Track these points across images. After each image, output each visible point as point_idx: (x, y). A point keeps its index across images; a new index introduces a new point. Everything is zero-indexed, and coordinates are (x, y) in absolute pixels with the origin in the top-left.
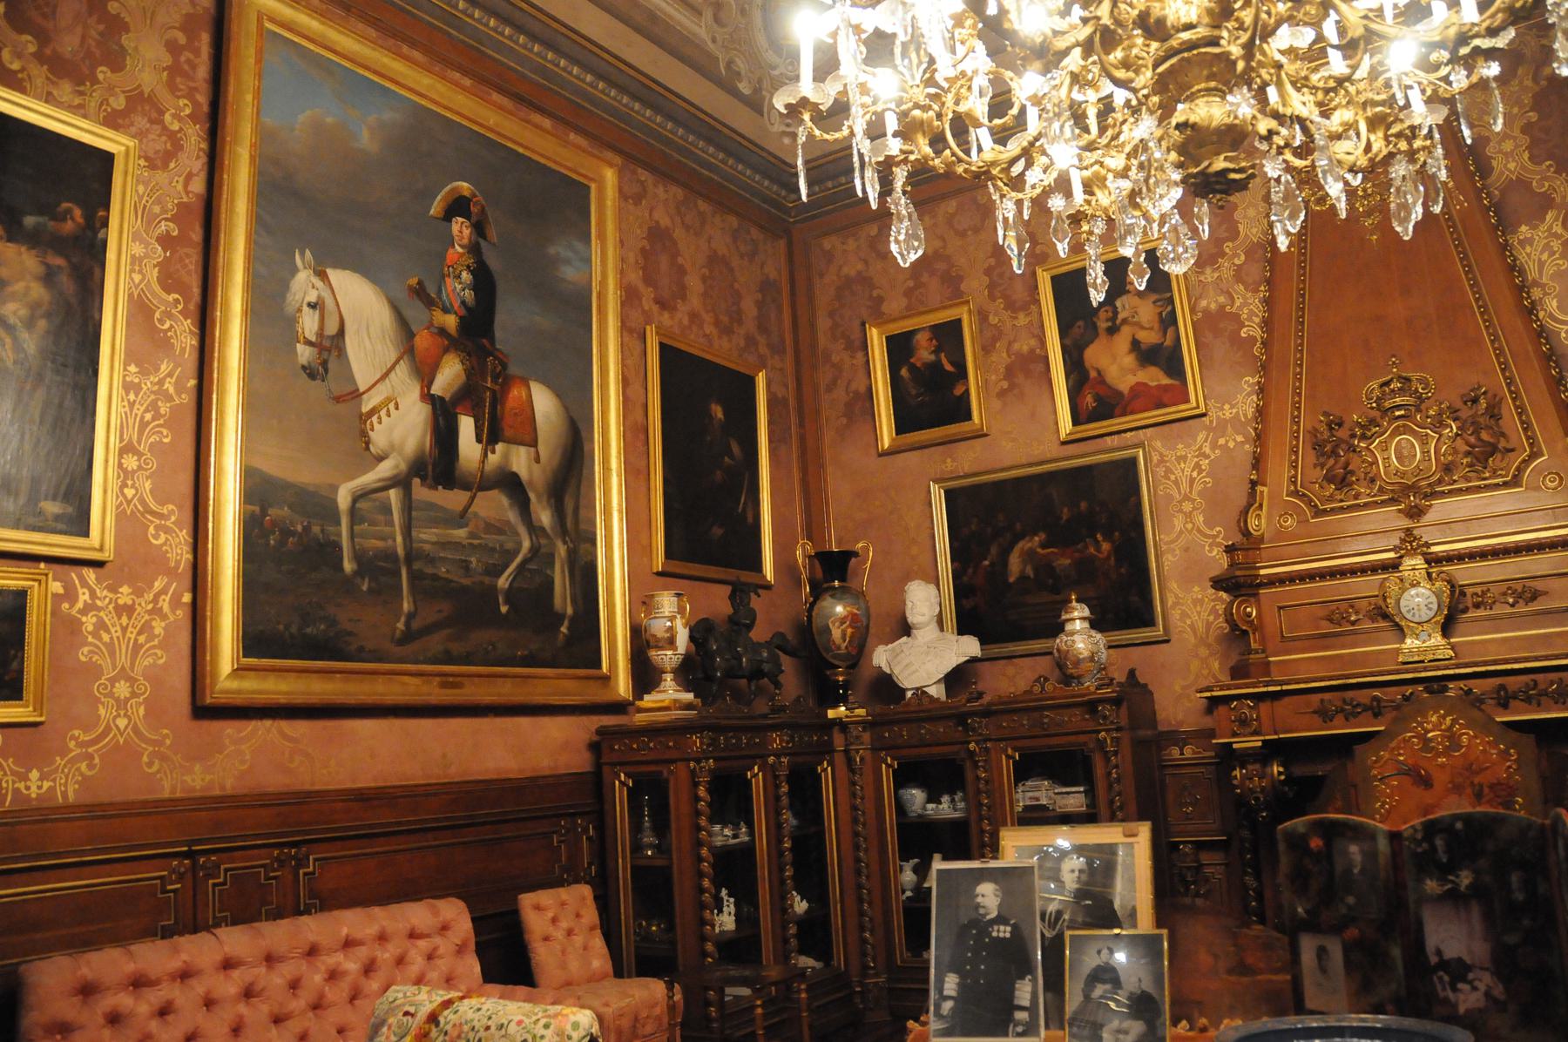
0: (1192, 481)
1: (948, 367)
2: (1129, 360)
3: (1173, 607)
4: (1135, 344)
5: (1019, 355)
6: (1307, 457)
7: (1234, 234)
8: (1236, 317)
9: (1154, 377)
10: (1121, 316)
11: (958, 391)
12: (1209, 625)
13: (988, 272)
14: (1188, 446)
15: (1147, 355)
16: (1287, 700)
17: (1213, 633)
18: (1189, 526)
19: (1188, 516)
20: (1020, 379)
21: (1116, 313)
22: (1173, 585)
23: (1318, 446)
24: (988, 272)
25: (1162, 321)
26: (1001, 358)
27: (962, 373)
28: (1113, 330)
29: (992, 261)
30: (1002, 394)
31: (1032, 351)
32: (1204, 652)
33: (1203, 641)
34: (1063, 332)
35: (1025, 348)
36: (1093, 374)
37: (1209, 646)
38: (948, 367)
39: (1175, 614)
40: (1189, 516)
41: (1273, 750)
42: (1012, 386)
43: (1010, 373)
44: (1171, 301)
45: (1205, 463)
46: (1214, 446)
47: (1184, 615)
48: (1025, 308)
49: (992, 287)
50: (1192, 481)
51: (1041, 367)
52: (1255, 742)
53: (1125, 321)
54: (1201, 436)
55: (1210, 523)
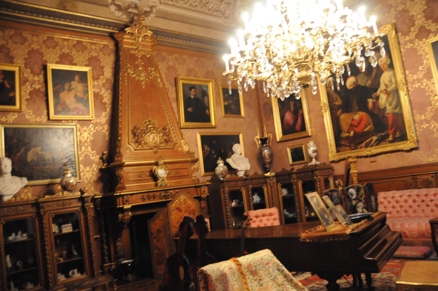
0: (88, 138)
1: (8, 86)
2: (74, 100)
3: (82, 172)
4: (76, 96)
5: (34, 88)
6: (131, 135)
7: (103, 75)
8: (102, 96)
9: (80, 106)
10: (72, 87)
11: (11, 95)
12: (91, 178)
13: (25, 59)
14: (87, 127)
15: (78, 99)
16: (135, 195)
17: (92, 180)
18: (87, 150)
19: (86, 147)
20: (34, 96)
21: (70, 86)
22: (81, 166)
23: (134, 134)
24: (25, 59)
25: (84, 91)
26: (28, 88)
27: (13, 88)
28: (70, 90)
29: (27, 56)
30: (27, 100)
31: (39, 89)
32: (89, 185)
33: (89, 182)
34: (54, 85)
35: (37, 87)
36: (62, 101)
37: (91, 184)
38: (8, 86)
39: (82, 174)
40: (86, 147)
41: (133, 209)
42: (31, 99)
43: (31, 93)
44: (87, 87)
45: (91, 133)
46: (94, 129)
47: (84, 175)
48: (38, 75)
49: (26, 65)
50: (88, 138)
51: (42, 95)
52: (129, 206)
53: (73, 88)
54: (91, 126)
55: (92, 150)
